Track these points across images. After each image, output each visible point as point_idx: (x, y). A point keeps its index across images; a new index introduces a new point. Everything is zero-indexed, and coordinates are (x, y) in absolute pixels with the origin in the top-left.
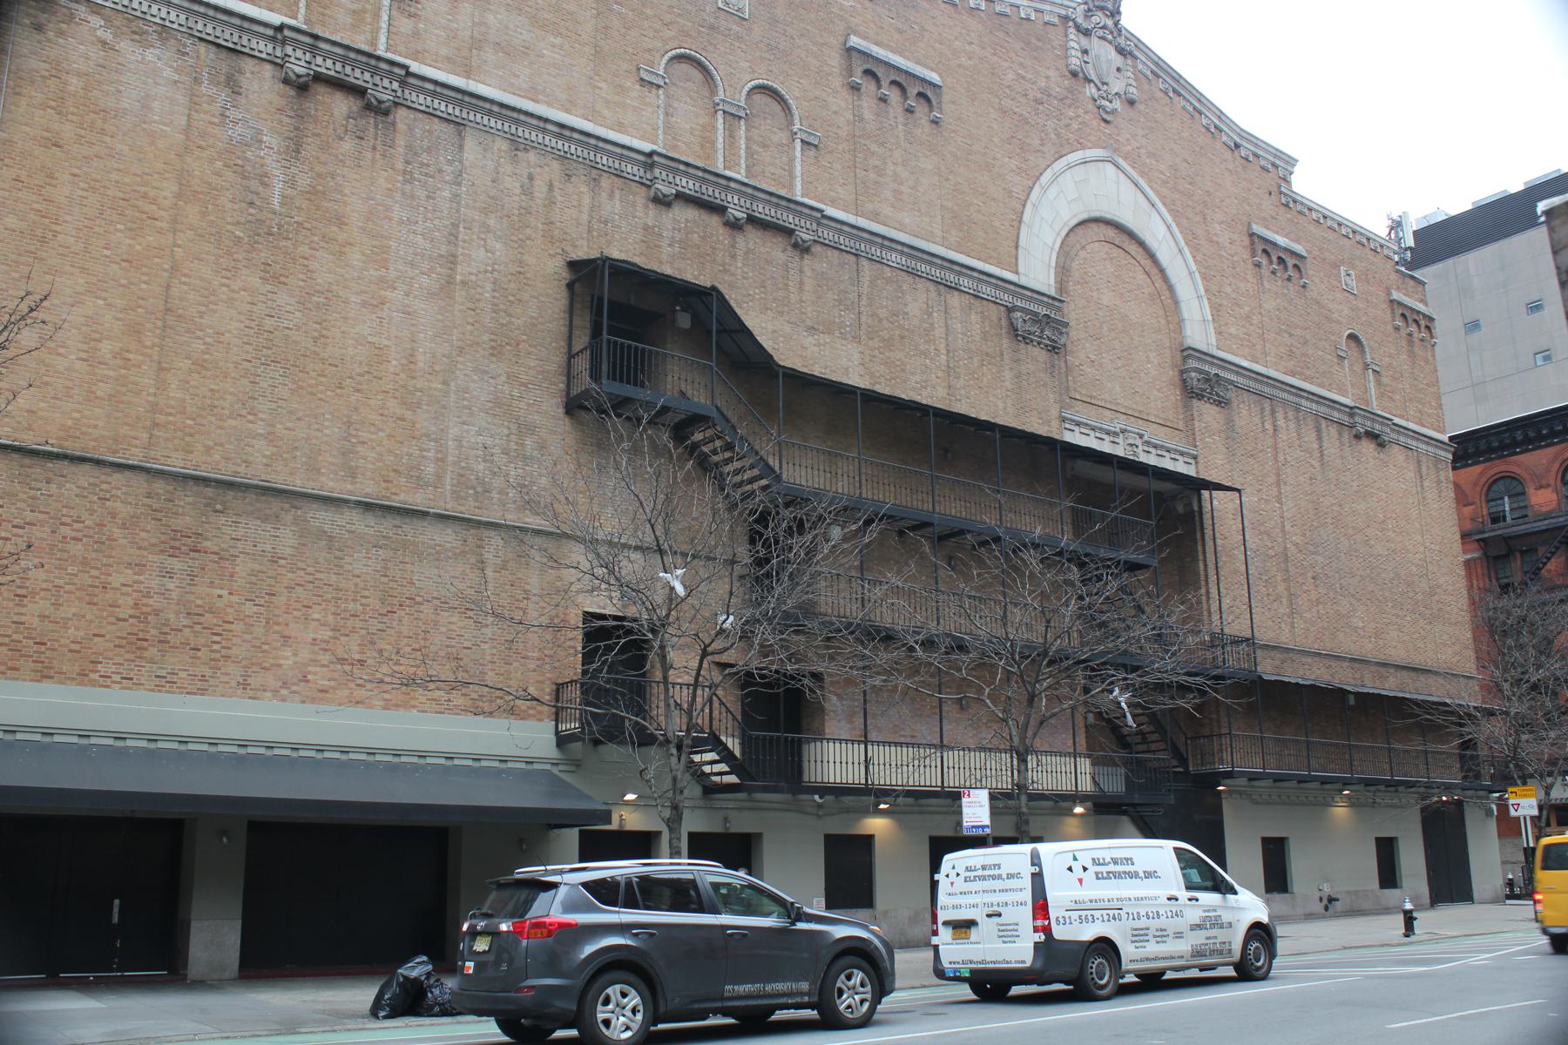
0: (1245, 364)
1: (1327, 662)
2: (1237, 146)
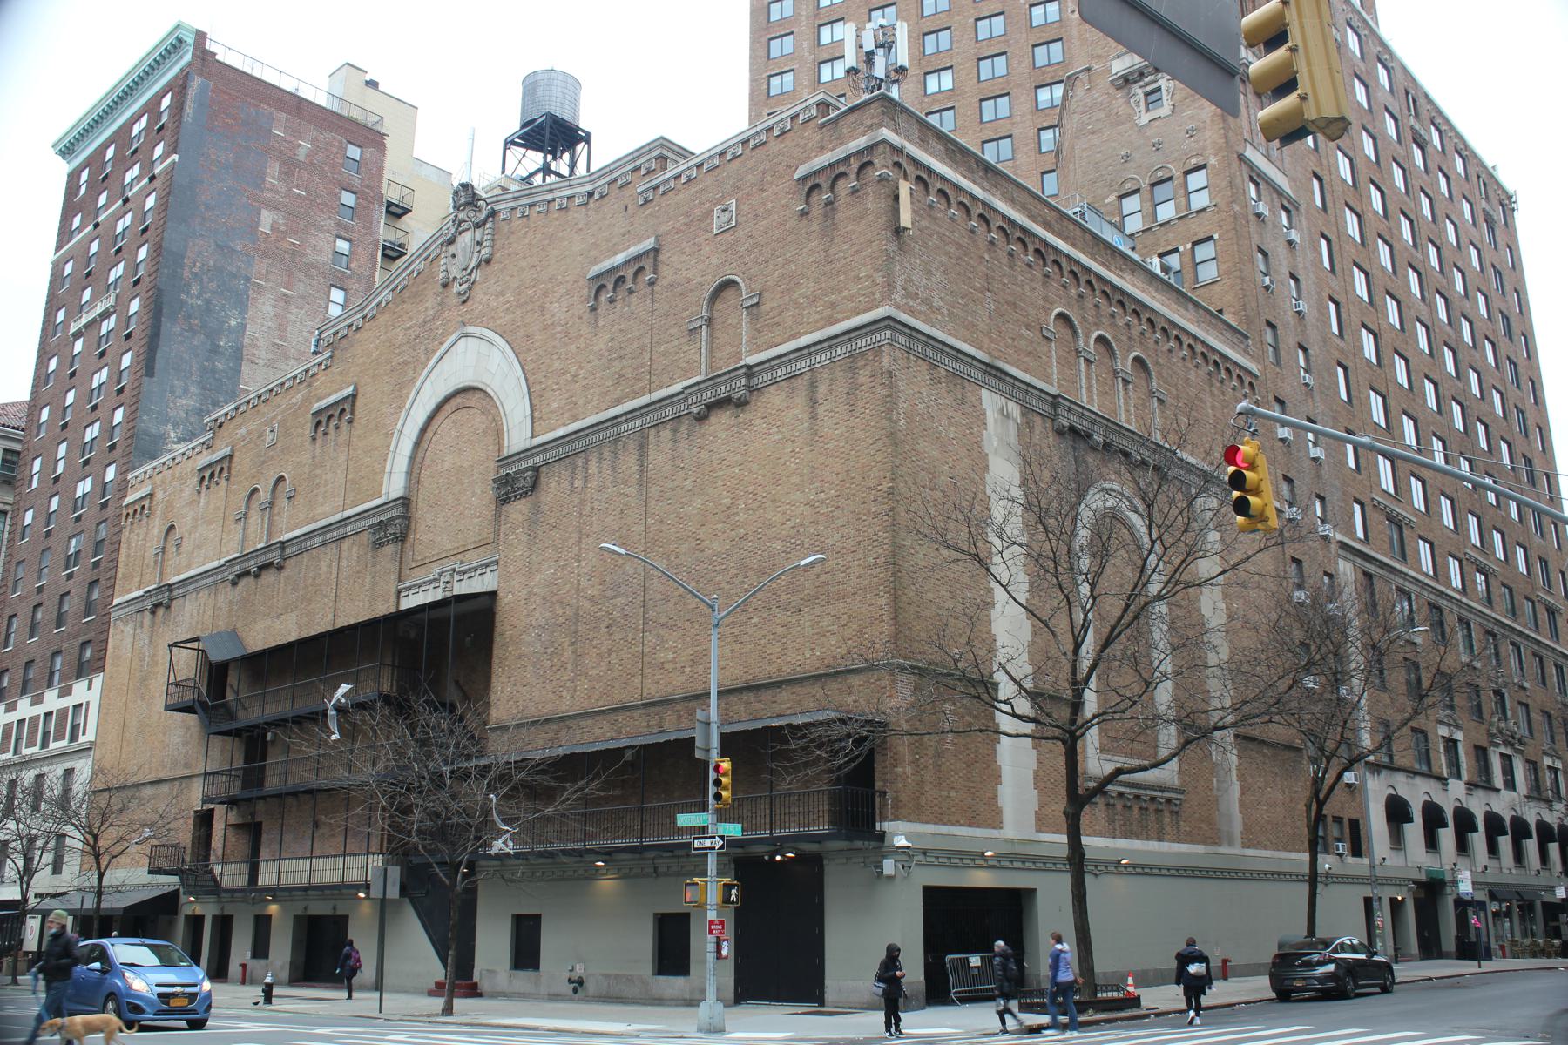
0: (560, 432)
1: (612, 717)
2: (591, 194)
